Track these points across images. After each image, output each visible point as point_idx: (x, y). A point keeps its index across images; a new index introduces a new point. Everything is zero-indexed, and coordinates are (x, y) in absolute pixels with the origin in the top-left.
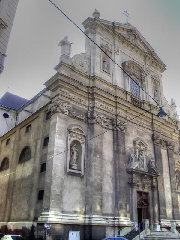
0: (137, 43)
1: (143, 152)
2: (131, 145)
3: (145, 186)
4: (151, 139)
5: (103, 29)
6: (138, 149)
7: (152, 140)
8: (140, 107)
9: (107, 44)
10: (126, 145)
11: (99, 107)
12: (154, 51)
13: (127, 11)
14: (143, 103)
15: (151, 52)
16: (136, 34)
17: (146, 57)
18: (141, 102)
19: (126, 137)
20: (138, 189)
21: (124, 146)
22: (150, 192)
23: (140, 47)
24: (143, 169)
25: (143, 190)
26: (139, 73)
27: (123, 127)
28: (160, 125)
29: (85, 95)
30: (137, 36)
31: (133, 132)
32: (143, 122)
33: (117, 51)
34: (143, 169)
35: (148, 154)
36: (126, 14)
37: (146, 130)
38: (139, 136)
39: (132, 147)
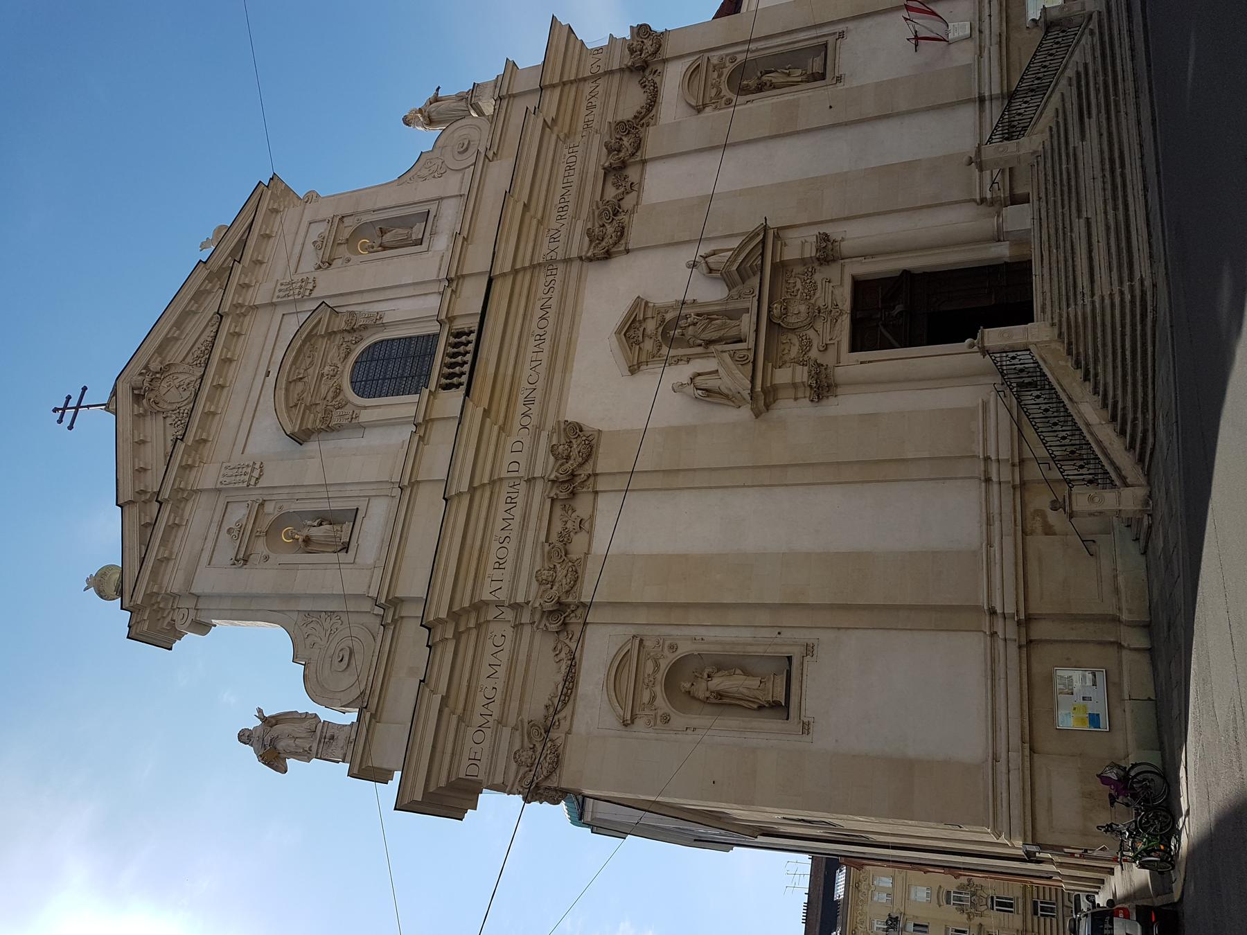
0: (189, 359)
5: (163, 561)
8: (473, 337)
9: (229, 531)
11: (507, 574)
12: (205, 263)
13: (55, 410)
14: (451, 319)
15: (209, 278)
16: (146, 367)
17: (241, 306)
18: (450, 334)
23: (201, 340)
24: (745, 317)
25: (841, 314)
26: (322, 344)
27: (574, 441)
29: (472, 643)
30: (155, 366)
33: (247, 478)
36: (68, 411)
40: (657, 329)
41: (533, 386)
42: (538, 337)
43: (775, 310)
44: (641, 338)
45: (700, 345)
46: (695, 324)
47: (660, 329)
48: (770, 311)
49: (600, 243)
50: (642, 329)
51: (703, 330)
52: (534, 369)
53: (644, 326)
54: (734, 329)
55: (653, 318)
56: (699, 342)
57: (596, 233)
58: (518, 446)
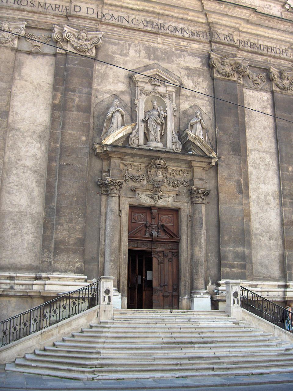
1: (166, 100)
2: (122, 87)
3: (163, 188)
4: (203, 65)
6: (143, 96)
7: (205, 68)
10: (95, 86)
19: (99, 68)
20: (136, 198)
21: (85, 90)
22: (185, 207)
24: (160, 145)
28: (237, 26)
31: (132, 53)
32: (174, 25)
34: (160, 145)
35: (185, 106)
37: (183, 43)
38: (152, 62)
39: (123, 92)
40: (159, 93)
41: (130, 21)
42: (162, 25)
43: (159, 161)
44: (153, 83)
45: (145, 118)
46: (159, 115)
47: (158, 95)
48: (159, 158)
49: (219, 62)
50: (160, 84)
51: (154, 120)
52: (142, 22)
53: (163, 86)
54: (154, 138)
55: (167, 91)
56: (147, 117)
57: (226, 60)
58: (90, 11)
